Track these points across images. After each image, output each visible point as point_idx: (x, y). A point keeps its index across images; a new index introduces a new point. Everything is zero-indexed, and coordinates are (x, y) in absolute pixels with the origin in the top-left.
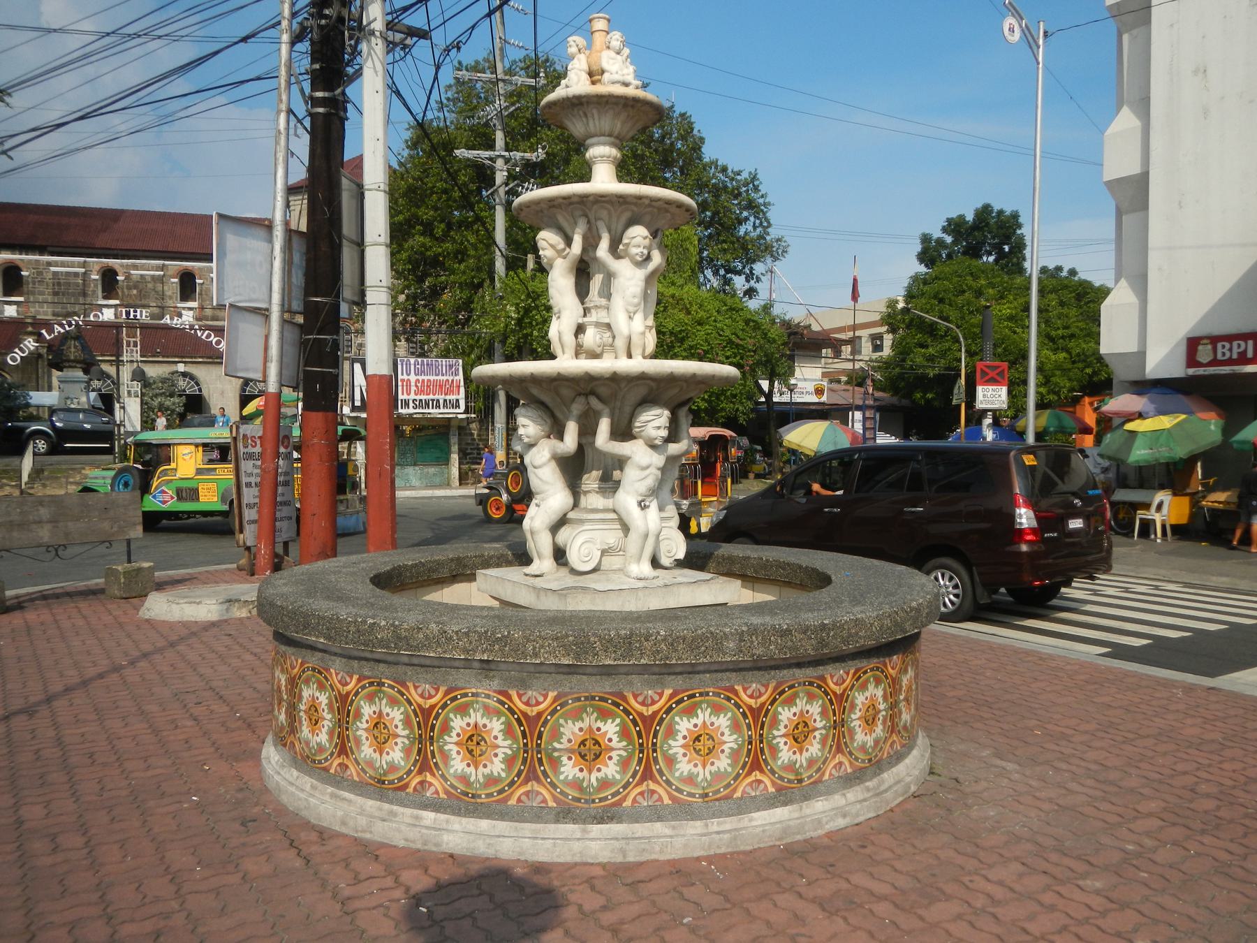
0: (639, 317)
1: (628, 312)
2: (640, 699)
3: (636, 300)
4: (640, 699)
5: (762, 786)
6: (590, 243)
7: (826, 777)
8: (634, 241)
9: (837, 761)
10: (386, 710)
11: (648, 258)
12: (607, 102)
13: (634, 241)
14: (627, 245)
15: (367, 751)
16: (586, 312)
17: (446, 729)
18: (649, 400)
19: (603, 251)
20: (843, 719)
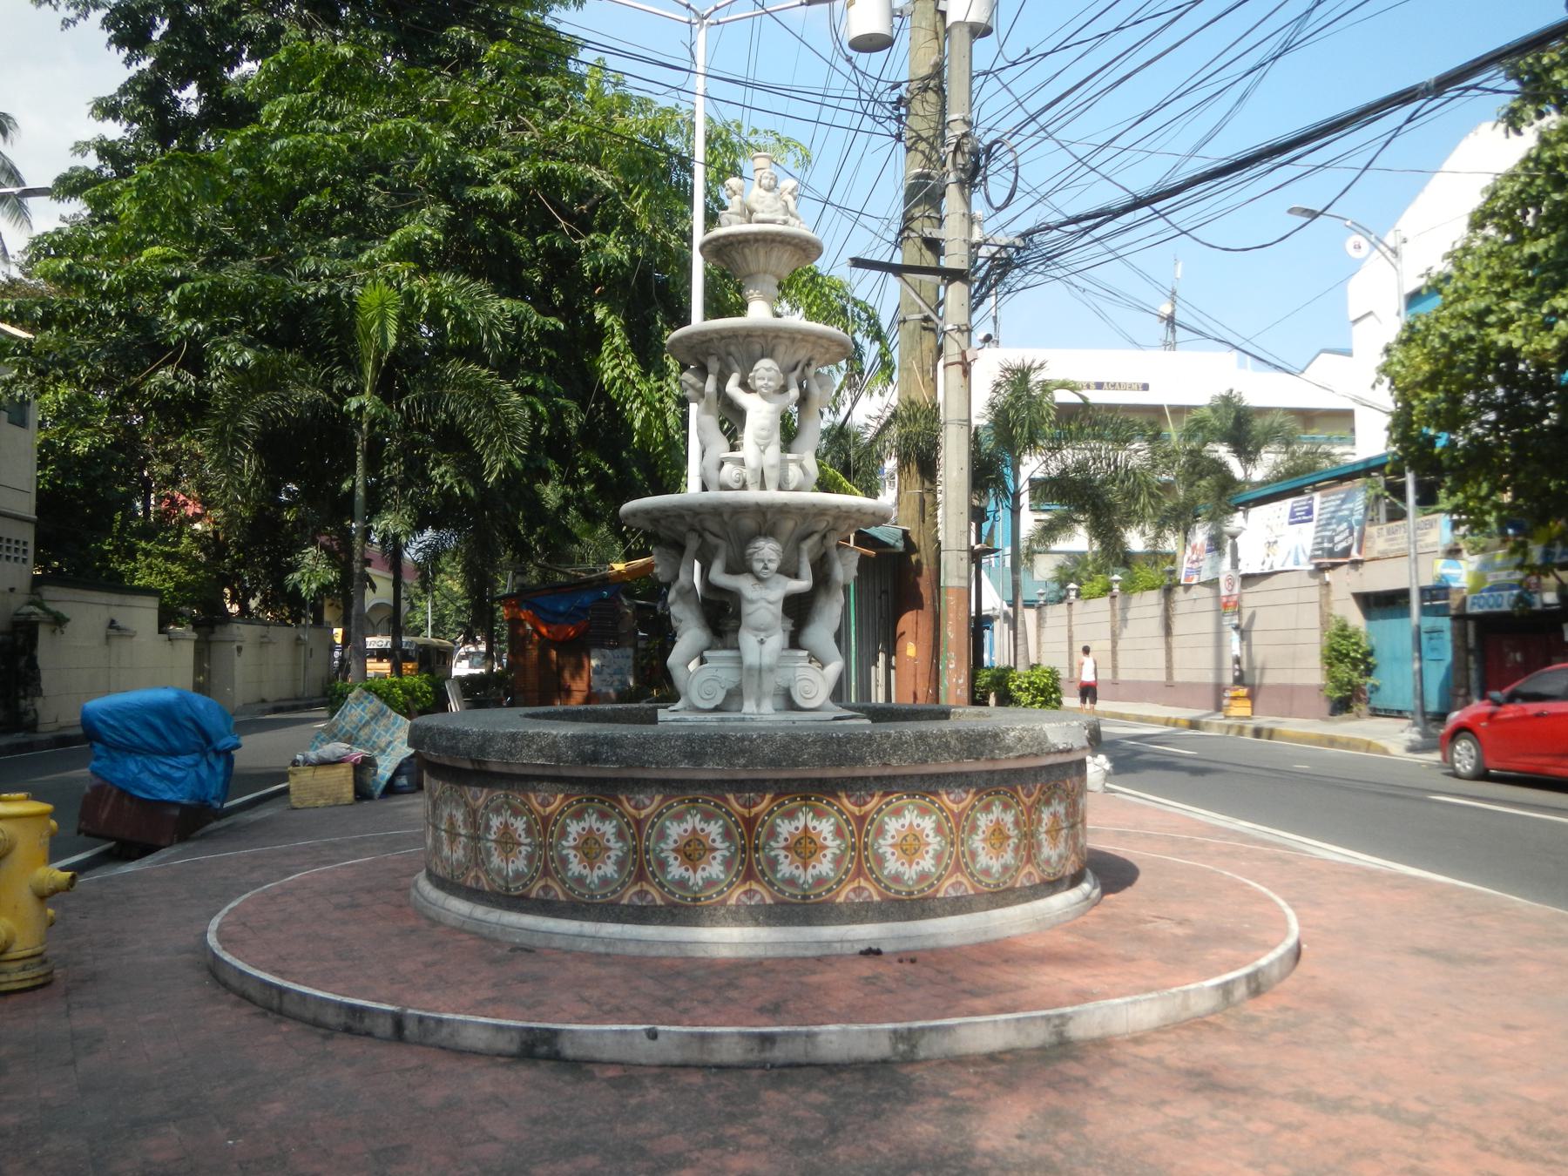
0: (773, 451)
1: (759, 445)
2: (632, 803)
3: (764, 433)
4: (632, 803)
5: (757, 898)
6: (722, 380)
7: (841, 899)
8: (758, 374)
9: (855, 884)
10: (454, 812)
11: (784, 389)
12: (773, 241)
13: (758, 374)
14: (754, 378)
15: (446, 851)
16: (733, 448)
17: (488, 828)
18: (768, 532)
19: (732, 387)
20: (866, 843)
